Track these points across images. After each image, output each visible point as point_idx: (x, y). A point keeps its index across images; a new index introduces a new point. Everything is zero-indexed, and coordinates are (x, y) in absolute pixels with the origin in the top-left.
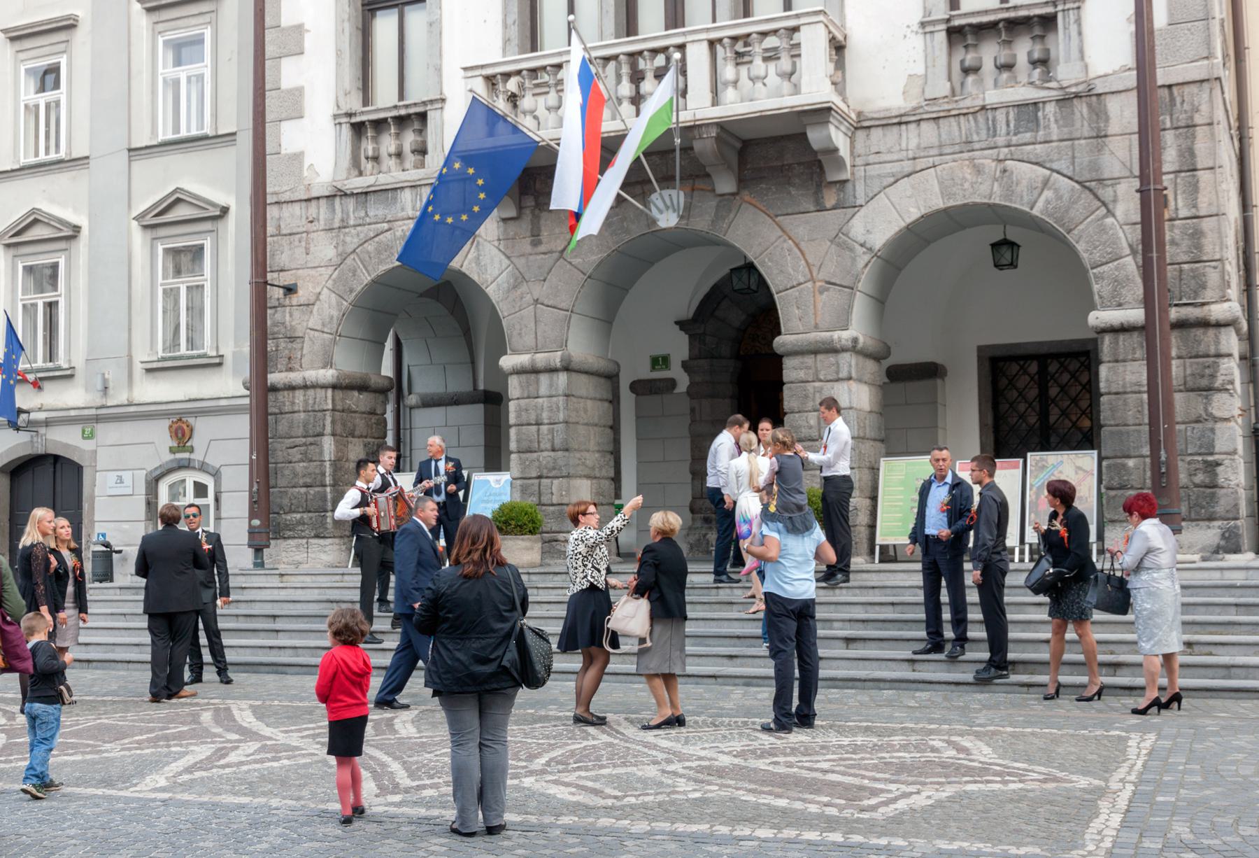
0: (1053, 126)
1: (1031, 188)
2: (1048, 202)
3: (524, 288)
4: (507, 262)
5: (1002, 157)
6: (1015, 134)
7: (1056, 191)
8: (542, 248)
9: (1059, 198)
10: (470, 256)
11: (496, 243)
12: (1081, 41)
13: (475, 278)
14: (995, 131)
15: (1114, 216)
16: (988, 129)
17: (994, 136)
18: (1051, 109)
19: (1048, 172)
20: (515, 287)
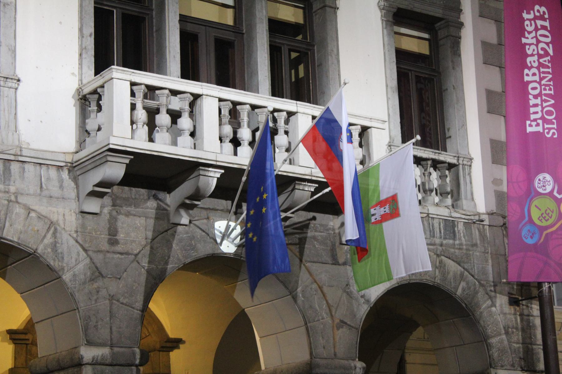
0: (463, 239)
1: (455, 277)
2: (464, 290)
3: (99, 283)
4: (82, 253)
5: (438, 253)
6: (445, 238)
7: (467, 283)
8: (119, 248)
9: (469, 288)
10: (46, 241)
11: (75, 235)
12: (472, 187)
13: (52, 263)
14: (434, 233)
15: (495, 306)
16: (430, 231)
17: (434, 237)
18: (461, 227)
19: (463, 270)
20: (92, 280)
